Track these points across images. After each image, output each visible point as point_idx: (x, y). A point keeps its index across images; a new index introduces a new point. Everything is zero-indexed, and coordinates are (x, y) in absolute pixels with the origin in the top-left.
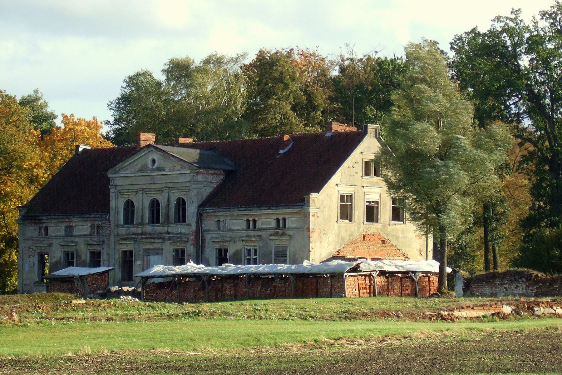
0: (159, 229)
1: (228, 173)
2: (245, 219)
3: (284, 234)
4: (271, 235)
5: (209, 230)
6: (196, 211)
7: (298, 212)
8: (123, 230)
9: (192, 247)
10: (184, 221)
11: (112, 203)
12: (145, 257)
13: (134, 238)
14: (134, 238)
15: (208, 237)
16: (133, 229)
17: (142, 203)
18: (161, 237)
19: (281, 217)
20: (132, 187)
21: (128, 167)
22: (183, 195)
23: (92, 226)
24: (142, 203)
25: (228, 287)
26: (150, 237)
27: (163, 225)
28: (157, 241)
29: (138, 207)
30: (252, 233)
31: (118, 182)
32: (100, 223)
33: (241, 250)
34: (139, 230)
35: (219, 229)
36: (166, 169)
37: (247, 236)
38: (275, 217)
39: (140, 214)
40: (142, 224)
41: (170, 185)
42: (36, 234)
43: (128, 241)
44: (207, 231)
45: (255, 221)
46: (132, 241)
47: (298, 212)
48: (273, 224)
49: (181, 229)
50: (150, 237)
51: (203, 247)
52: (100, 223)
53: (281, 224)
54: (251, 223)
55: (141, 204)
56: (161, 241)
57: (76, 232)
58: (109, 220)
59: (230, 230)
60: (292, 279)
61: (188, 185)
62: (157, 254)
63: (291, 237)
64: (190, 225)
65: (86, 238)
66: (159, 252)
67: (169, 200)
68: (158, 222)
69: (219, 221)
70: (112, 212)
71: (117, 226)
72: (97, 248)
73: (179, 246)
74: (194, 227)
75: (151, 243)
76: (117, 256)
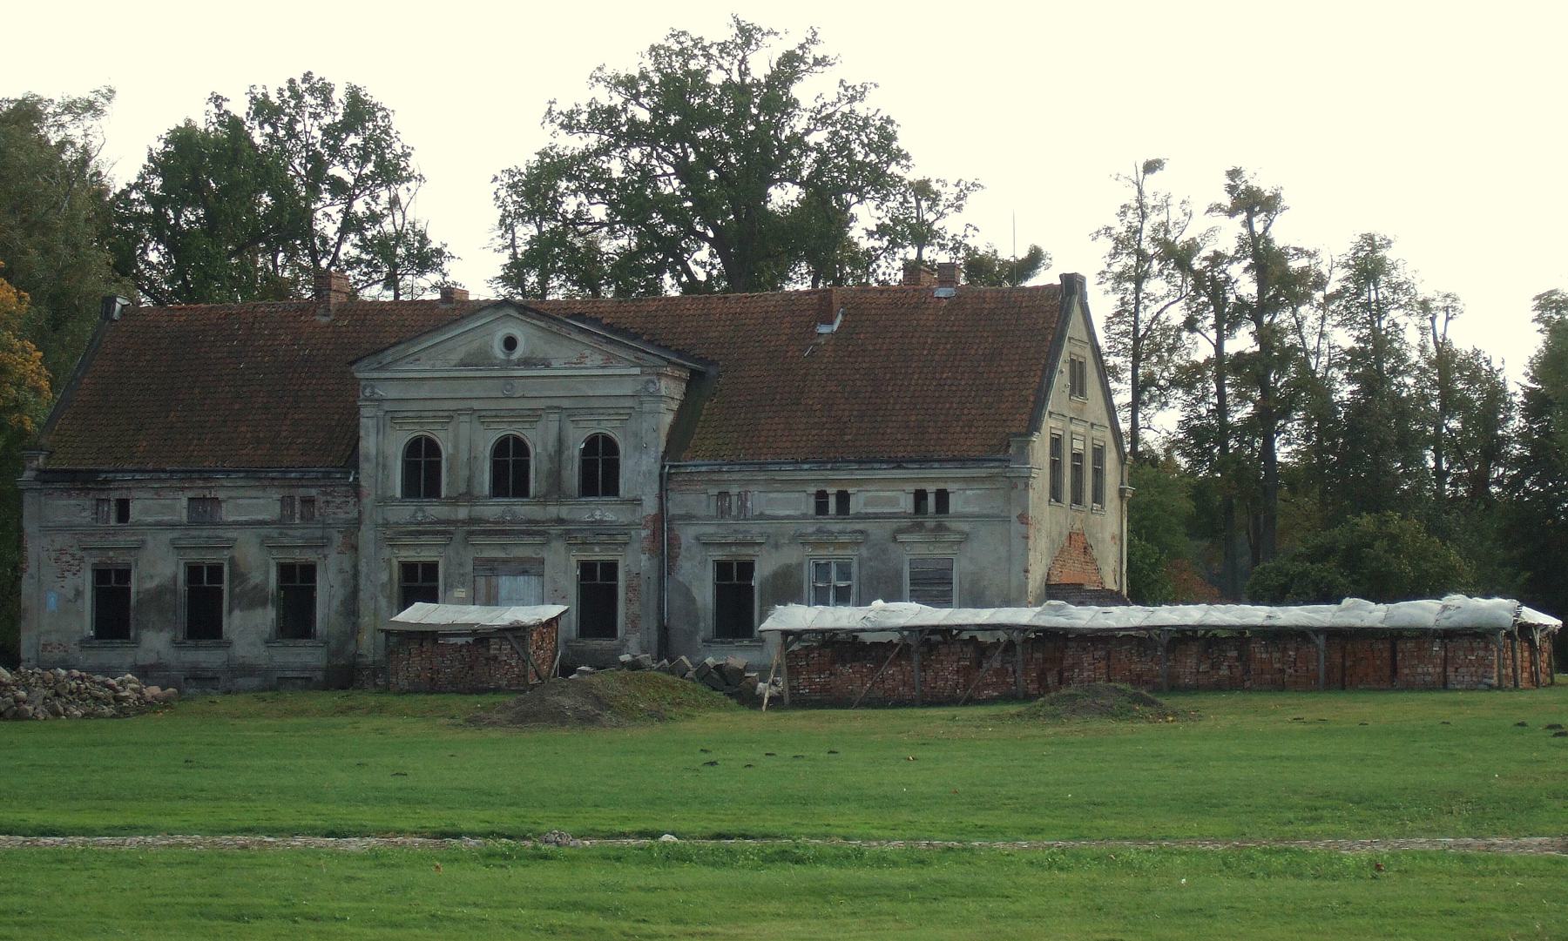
0: (523, 509)
1: (695, 381)
2: (813, 489)
3: (940, 528)
4: (900, 531)
5: (689, 518)
6: (656, 469)
7: (990, 478)
8: (404, 513)
9: (644, 557)
10: (611, 488)
11: (368, 444)
12: (481, 582)
13: (443, 531)
14: (443, 531)
15: (687, 534)
16: (435, 510)
17: (467, 449)
18: (534, 530)
19: (931, 488)
20: (429, 405)
21: (423, 355)
22: (606, 428)
23: (286, 502)
24: (467, 449)
25: (1087, 660)
26: (499, 531)
27: (454, 501)
28: (529, 540)
29: (453, 459)
30: (835, 527)
31: (391, 391)
32: (313, 492)
33: (800, 565)
34: (462, 513)
35: (723, 512)
36: (555, 364)
37: (819, 531)
38: (912, 488)
39: (464, 473)
40: (469, 497)
41: (566, 403)
42: (86, 516)
43: (424, 539)
44: (681, 517)
45: (843, 498)
46: (440, 540)
47: (990, 478)
48: (906, 504)
49: (604, 511)
50: (499, 531)
51: (673, 558)
52: (313, 492)
53: (931, 507)
54: (832, 501)
55: (464, 447)
56: (538, 540)
57: (228, 513)
58: (356, 489)
59: (761, 516)
60: (1321, 641)
61: (628, 403)
62: (525, 572)
63: (966, 537)
64: (636, 502)
65: (264, 531)
66: (525, 568)
67: (560, 441)
68: (521, 490)
69: (723, 495)
70: (366, 468)
71: (384, 501)
72: (309, 556)
73: (598, 555)
74: (650, 507)
75: (503, 546)
76: (384, 577)
